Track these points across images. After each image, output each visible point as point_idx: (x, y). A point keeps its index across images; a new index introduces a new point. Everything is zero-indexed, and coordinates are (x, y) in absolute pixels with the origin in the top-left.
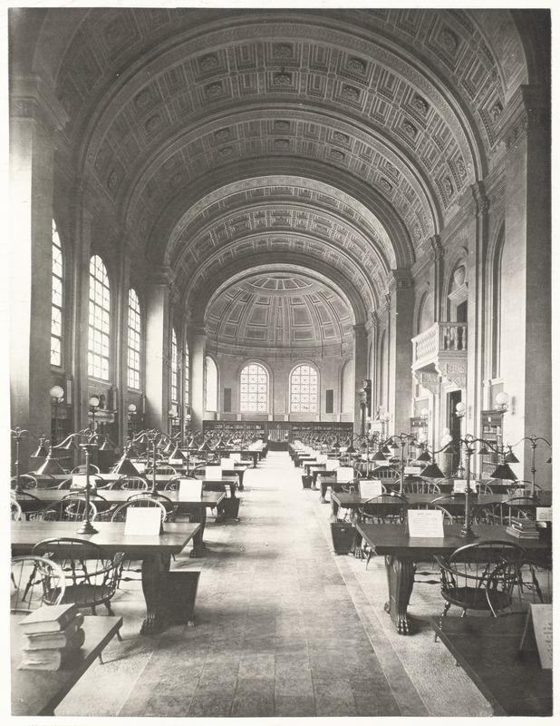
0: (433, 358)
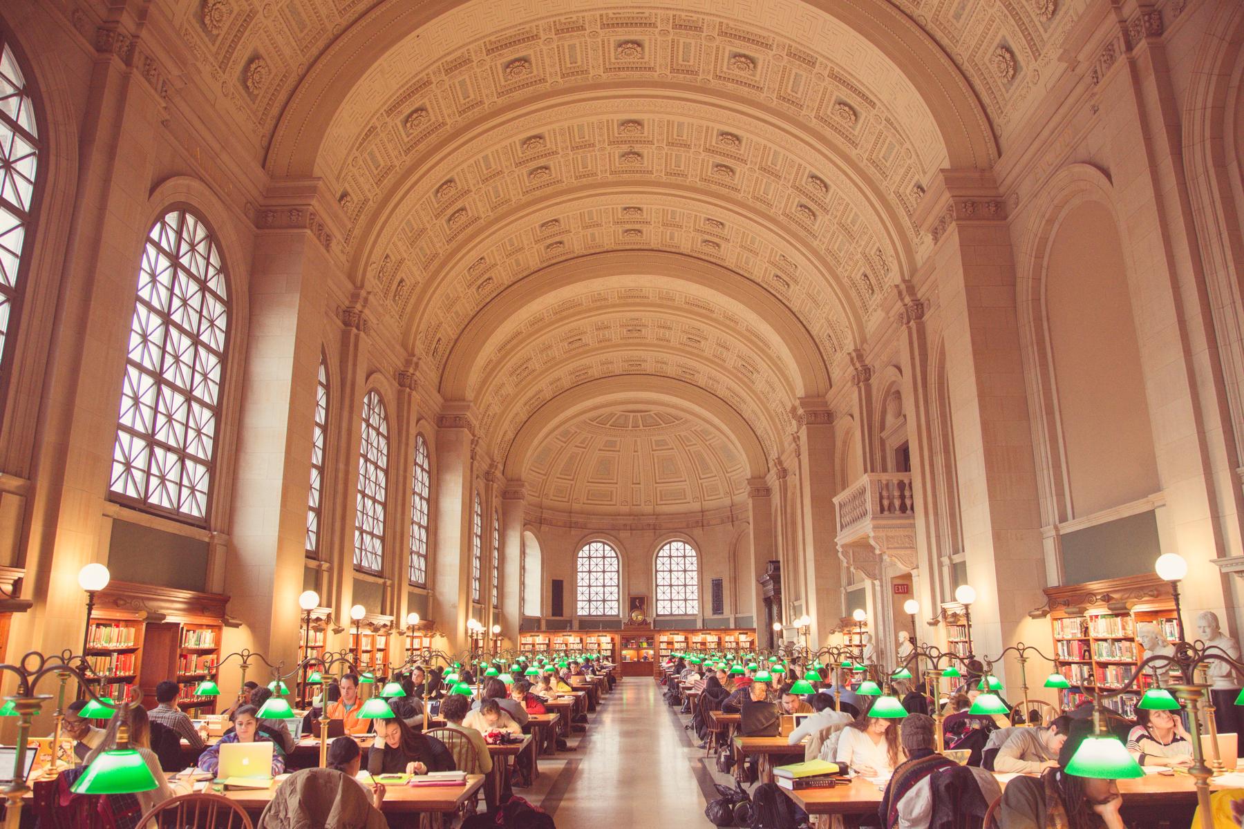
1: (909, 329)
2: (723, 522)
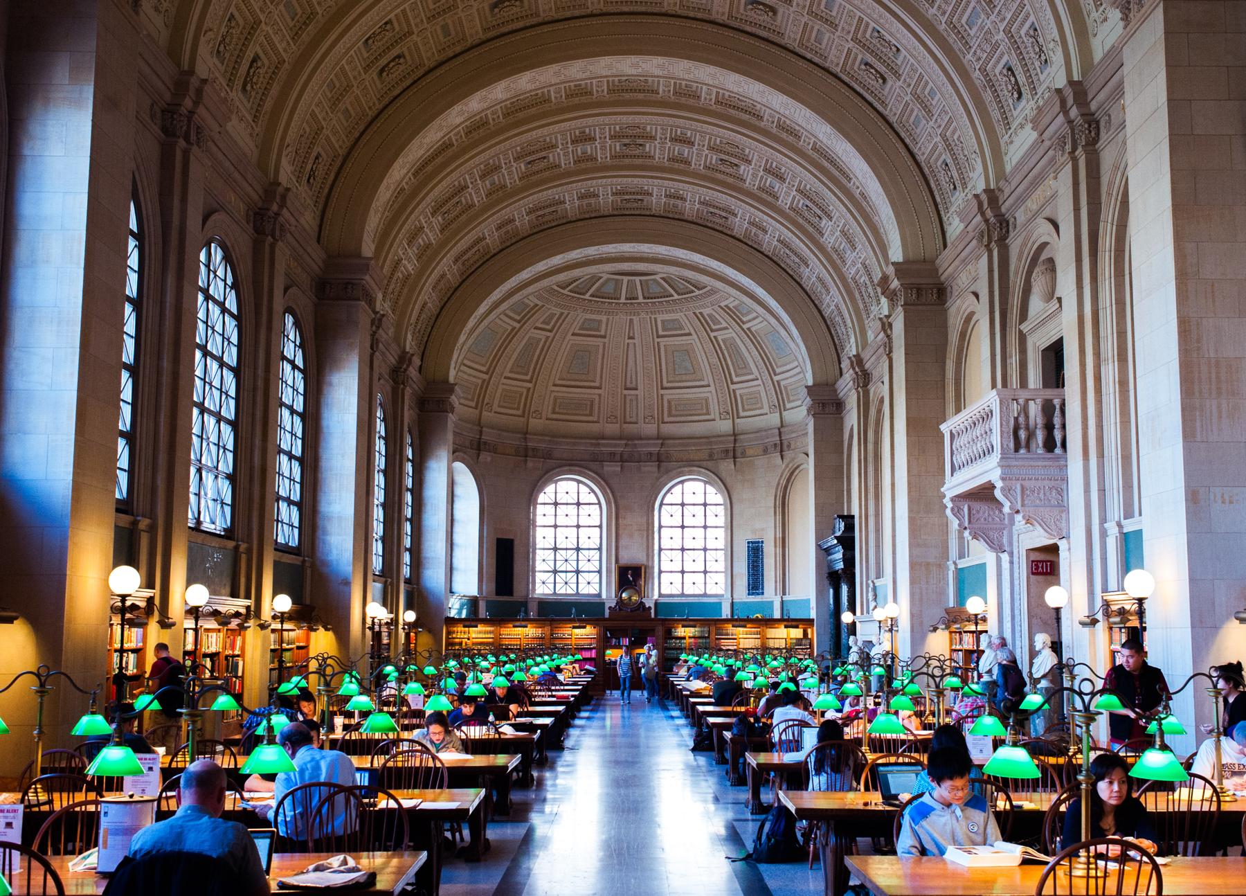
0: (989, 470)
2: (765, 451)
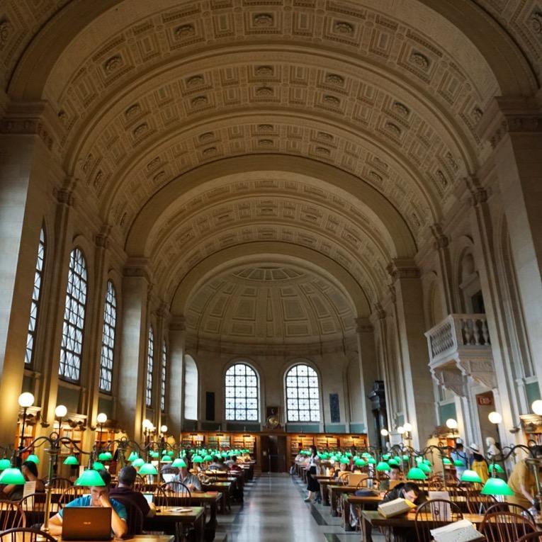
1: (477, 209)
